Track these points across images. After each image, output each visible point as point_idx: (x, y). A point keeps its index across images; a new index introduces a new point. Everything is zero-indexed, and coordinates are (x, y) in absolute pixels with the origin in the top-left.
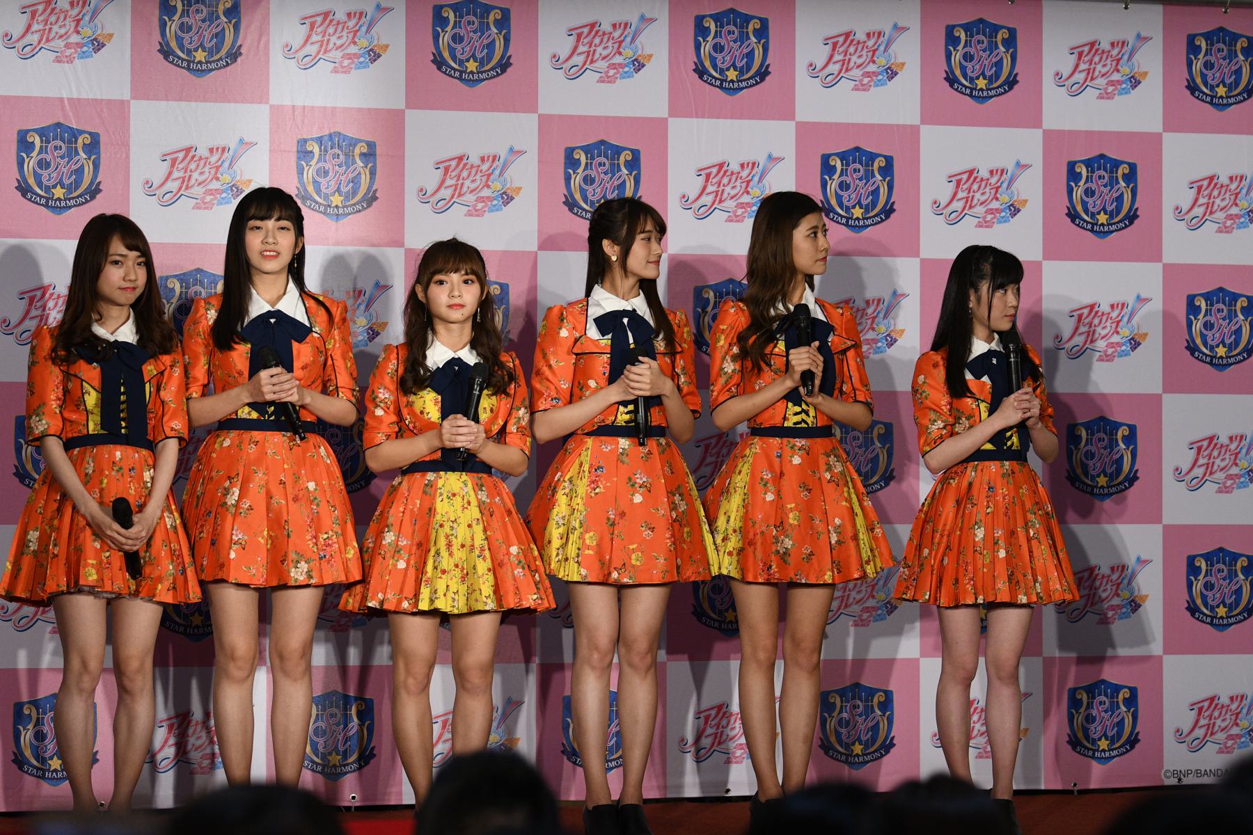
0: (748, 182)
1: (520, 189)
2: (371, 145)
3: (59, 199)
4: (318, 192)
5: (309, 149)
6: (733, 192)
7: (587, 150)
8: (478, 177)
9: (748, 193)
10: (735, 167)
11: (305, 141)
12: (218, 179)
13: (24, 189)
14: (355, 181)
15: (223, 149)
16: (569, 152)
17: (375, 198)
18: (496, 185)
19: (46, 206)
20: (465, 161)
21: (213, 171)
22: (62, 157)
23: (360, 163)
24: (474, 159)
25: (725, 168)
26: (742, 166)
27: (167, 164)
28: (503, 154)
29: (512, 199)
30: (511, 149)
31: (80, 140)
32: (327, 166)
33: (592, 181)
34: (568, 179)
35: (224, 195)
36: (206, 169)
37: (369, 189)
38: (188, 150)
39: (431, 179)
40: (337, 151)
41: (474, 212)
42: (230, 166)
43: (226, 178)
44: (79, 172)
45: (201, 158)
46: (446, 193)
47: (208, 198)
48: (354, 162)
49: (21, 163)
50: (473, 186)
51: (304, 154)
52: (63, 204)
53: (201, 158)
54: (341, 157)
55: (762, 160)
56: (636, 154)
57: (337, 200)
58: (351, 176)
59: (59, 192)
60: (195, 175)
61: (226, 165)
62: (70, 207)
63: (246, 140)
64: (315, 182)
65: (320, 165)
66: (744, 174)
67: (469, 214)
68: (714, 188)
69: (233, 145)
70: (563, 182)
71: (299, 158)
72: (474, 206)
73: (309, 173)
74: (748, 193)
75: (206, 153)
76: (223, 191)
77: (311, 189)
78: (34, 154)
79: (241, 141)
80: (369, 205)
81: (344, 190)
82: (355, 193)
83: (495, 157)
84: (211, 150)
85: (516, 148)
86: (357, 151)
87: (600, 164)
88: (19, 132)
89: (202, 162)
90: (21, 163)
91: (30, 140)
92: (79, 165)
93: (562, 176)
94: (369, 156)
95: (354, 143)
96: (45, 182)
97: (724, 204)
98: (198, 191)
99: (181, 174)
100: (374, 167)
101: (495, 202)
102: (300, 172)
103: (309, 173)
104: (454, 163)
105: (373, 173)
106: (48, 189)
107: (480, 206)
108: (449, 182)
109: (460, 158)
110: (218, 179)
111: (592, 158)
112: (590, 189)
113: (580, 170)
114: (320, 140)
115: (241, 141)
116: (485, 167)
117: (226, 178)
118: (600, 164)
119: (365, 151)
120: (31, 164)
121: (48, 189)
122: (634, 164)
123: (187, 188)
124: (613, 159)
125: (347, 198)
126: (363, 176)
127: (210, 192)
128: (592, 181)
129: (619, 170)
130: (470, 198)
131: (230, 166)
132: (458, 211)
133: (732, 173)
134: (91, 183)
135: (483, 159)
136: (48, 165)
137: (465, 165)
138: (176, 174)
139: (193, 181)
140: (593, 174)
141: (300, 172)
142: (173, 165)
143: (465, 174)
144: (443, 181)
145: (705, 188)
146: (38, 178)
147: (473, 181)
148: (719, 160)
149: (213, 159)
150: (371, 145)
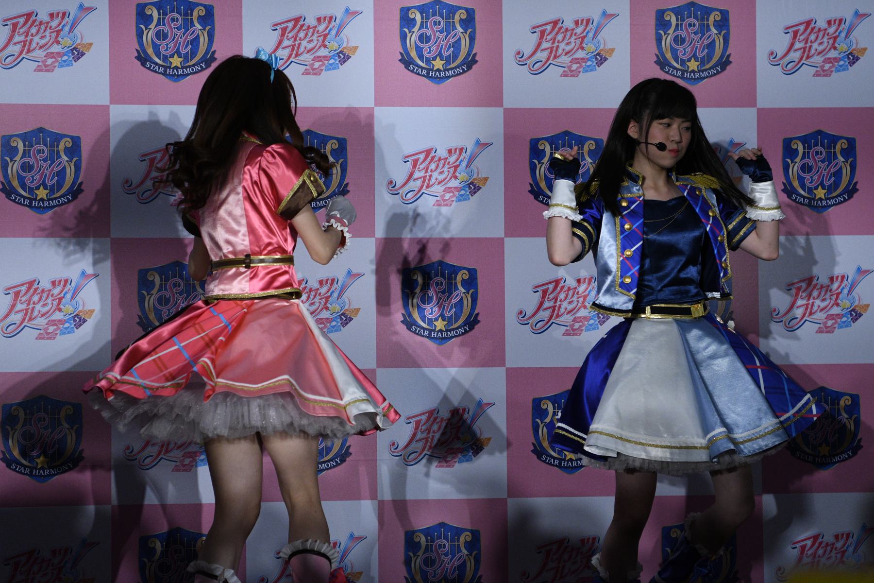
0: (835, 38)
1: (613, 50)
2: (470, 13)
3: (177, 68)
4: (421, 57)
5: (412, 16)
6: (821, 48)
7: (677, 11)
8: (572, 40)
9: (835, 48)
10: (822, 24)
11: (408, 9)
12: (325, 46)
13: (143, 59)
14: (457, 45)
15: (331, 18)
16: (660, 14)
17: (474, 61)
18: (590, 47)
19: (165, 74)
20: (560, 25)
21: (321, 39)
22: (179, 29)
23: (460, 29)
24: (569, 23)
25: (813, 25)
26: (829, 22)
27: (277, 34)
28: (596, 17)
29: (606, 59)
30: (604, 14)
31: (195, 13)
32: (429, 32)
33: (683, 41)
34: (659, 40)
35: (332, 61)
36: (315, 37)
37: (468, 55)
38: (297, 20)
39: (528, 43)
40: (438, 18)
41: (569, 73)
42: (337, 34)
43: (333, 45)
44: (195, 42)
45: (309, 27)
46: (542, 55)
47: (317, 65)
48: (454, 28)
49: (140, 34)
50: (568, 48)
51: (406, 21)
52: (180, 72)
53: (309, 27)
54: (442, 23)
55: (849, 16)
56: (725, 14)
57: (438, 64)
58: (452, 41)
59: (176, 61)
60: (304, 43)
61: (334, 32)
62: (188, 75)
63: (352, 9)
64: (417, 47)
65: (422, 31)
66: (831, 30)
67: (564, 75)
68: (802, 45)
69: (339, 14)
70: (654, 42)
71: (401, 27)
72: (569, 67)
73: (413, 39)
74: (835, 48)
75: (313, 23)
76: (330, 58)
77: (413, 54)
78: (152, 26)
79: (347, 10)
80: (469, 68)
81: (445, 54)
82: (455, 56)
83: (588, 21)
84: (319, 19)
85: (609, 12)
86: (457, 18)
87: (690, 25)
88: (138, 5)
89: (311, 31)
90: (140, 34)
91: (149, 13)
92: (193, 36)
93: (654, 37)
94: (469, 22)
95: (453, 10)
96: (163, 52)
97: (811, 60)
98: (307, 58)
99: (290, 42)
100: (474, 32)
101: (589, 63)
102: (403, 37)
103: (413, 39)
104: (549, 27)
105: (472, 38)
106: (165, 58)
107: (575, 67)
108: (545, 45)
109: (555, 23)
110: (325, 46)
111: (683, 20)
112: (680, 48)
113: (671, 31)
114: (422, 9)
115: (347, 10)
116: (579, 30)
117: (333, 45)
118: (690, 25)
119: (464, 17)
120: (149, 35)
121: (165, 58)
122: (723, 24)
123: (297, 55)
124: (702, 19)
125: (448, 61)
126: (463, 42)
127: (318, 59)
128: (683, 41)
129: (709, 29)
130: (565, 60)
131: (337, 34)
132: (553, 72)
133: (820, 30)
134: (207, 53)
135: (577, 23)
136: (165, 37)
137: (561, 28)
138: (286, 43)
139: (302, 49)
140: (684, 34)
141: (403, 37)
142: (283, 35)
143: (560, 37)
144: (539, 45)
145: (792, 45)
146: (156, 48)
147: (568, 44)
148: (806, 18)
149: (321, 28)
150: (470, 13)
